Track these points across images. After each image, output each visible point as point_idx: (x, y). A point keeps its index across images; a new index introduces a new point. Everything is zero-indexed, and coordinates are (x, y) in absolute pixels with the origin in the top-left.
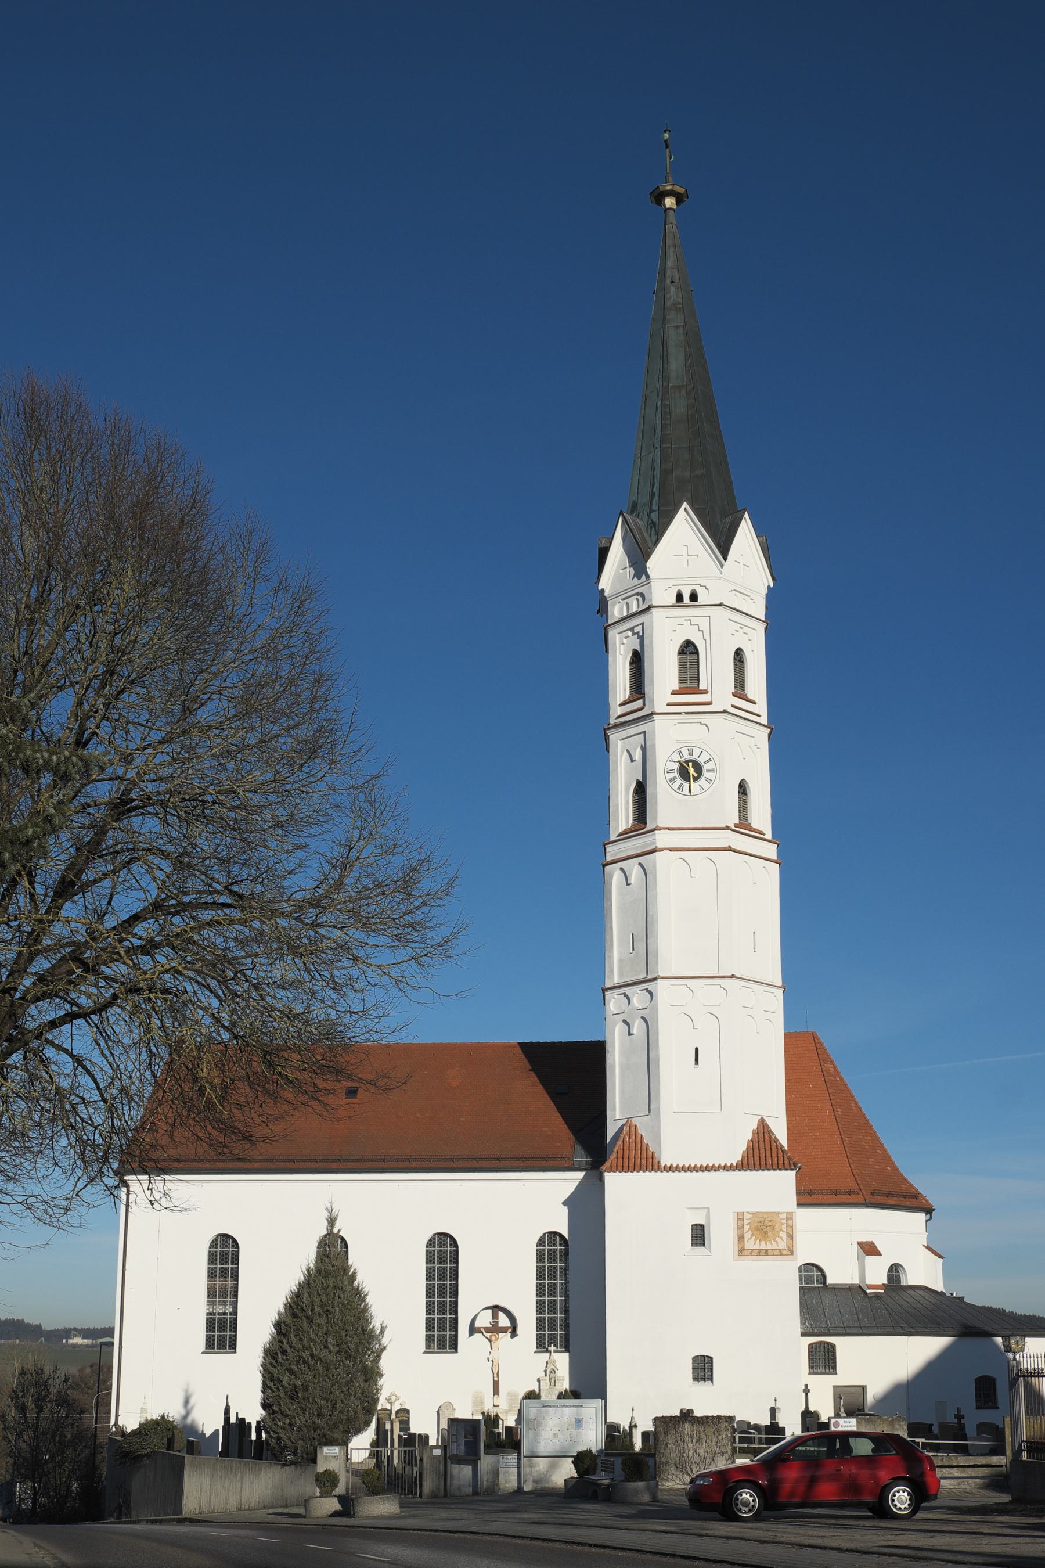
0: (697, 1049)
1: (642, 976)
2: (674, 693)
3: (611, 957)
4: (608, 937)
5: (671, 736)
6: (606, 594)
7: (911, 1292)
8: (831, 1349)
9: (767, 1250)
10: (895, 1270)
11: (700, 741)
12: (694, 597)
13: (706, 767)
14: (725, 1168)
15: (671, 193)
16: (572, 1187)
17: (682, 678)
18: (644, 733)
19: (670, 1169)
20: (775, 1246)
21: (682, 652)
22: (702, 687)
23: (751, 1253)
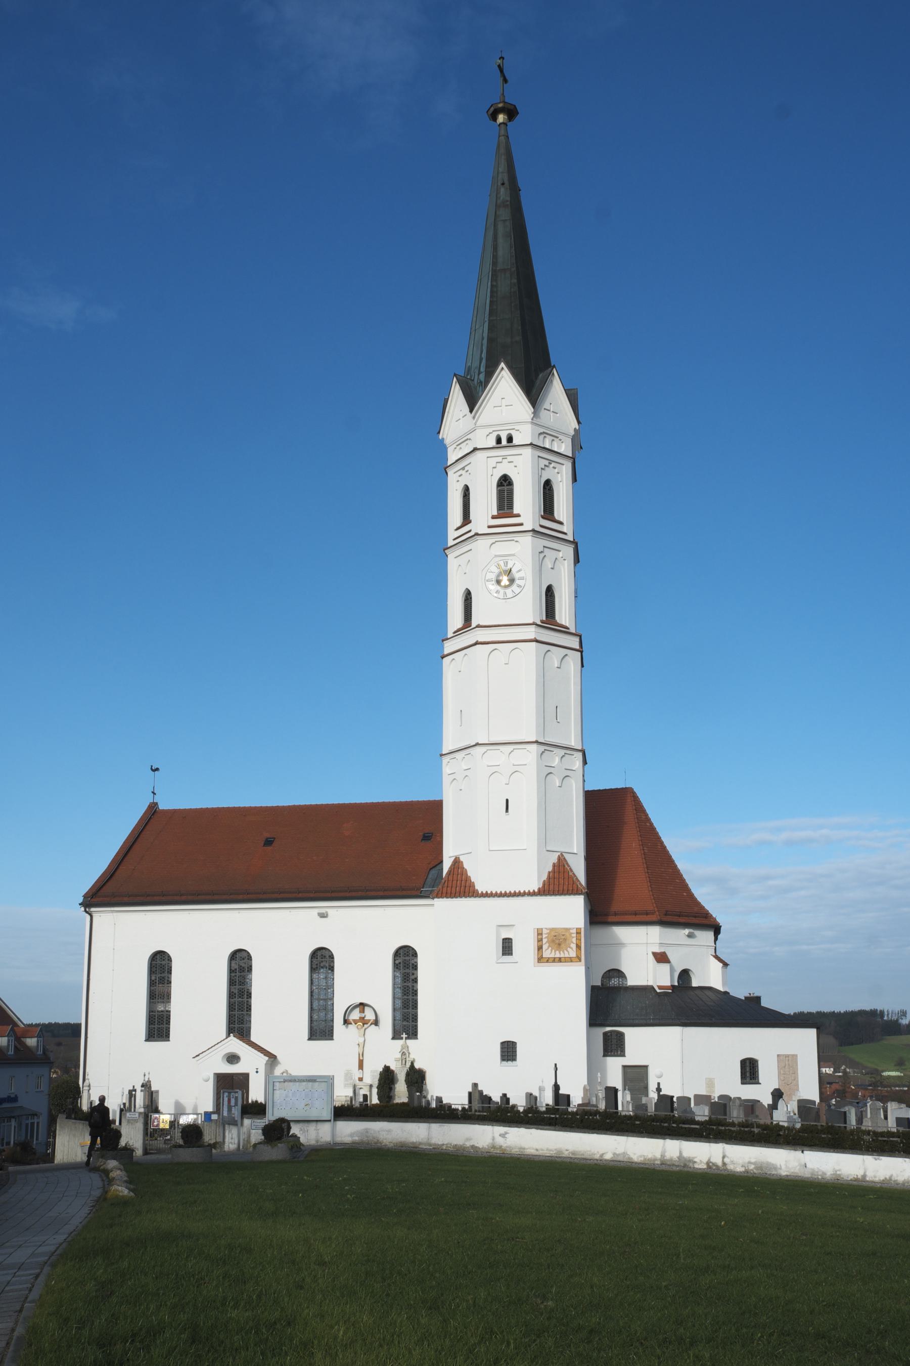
0: (507, 800)
2: (494, 517)
7: (698, 992)
8: (621, 1036)
9: (560, 958)
10: (685, 974)
11: (513, 555)
12: (510, 439)
17: (500, 507)
22: (515, 511)
23: (547, 960)
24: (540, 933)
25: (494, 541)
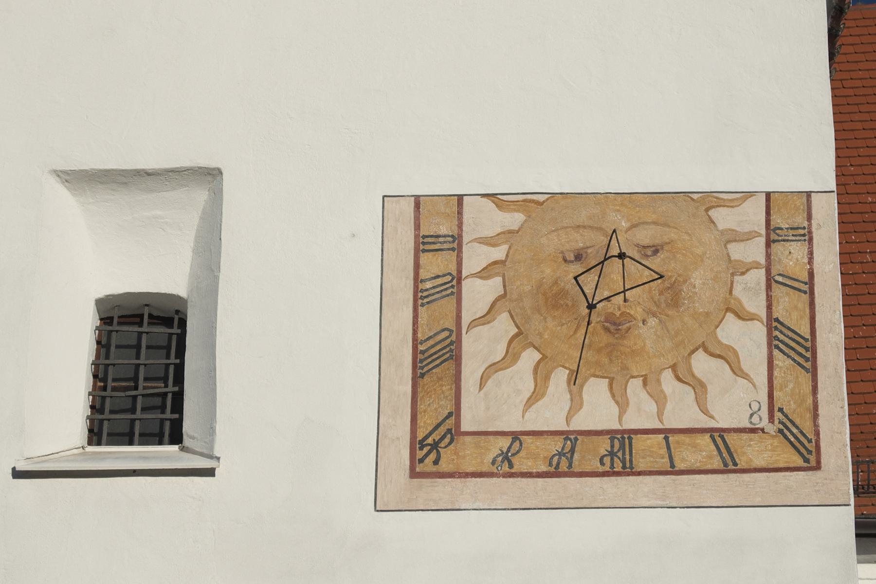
20: (682, 411)
24: (433, 233)
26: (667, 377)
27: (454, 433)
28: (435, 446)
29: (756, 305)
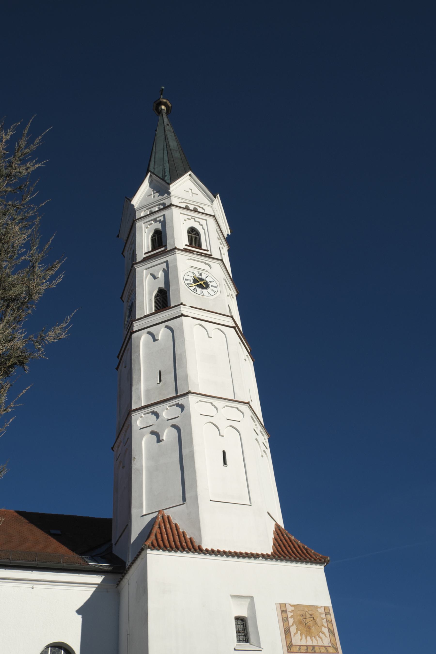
0: (224, 452)
1: (174, 395)
3: (139, 389)
4: (134, 376)
5: (185, 265)
6: (135, 207)
9: (313, 647)
13: (211, 284)
14: (265, 557)
15: (165, 104)
16: (86, 593)
18: (167, 262)
19: (212, 552)
20: (320, 644)
21: (189, 232)
22: (204, 247)
24: (283, 609)
25: (190, 258)
26: (317, 636)
27: (292, 645)
28: (290, 647)
29: (326, 625)
